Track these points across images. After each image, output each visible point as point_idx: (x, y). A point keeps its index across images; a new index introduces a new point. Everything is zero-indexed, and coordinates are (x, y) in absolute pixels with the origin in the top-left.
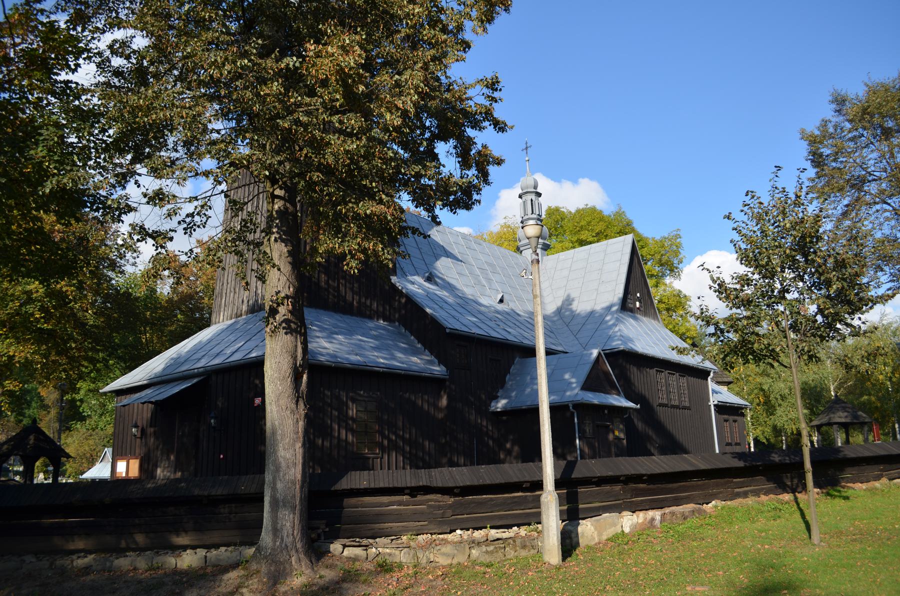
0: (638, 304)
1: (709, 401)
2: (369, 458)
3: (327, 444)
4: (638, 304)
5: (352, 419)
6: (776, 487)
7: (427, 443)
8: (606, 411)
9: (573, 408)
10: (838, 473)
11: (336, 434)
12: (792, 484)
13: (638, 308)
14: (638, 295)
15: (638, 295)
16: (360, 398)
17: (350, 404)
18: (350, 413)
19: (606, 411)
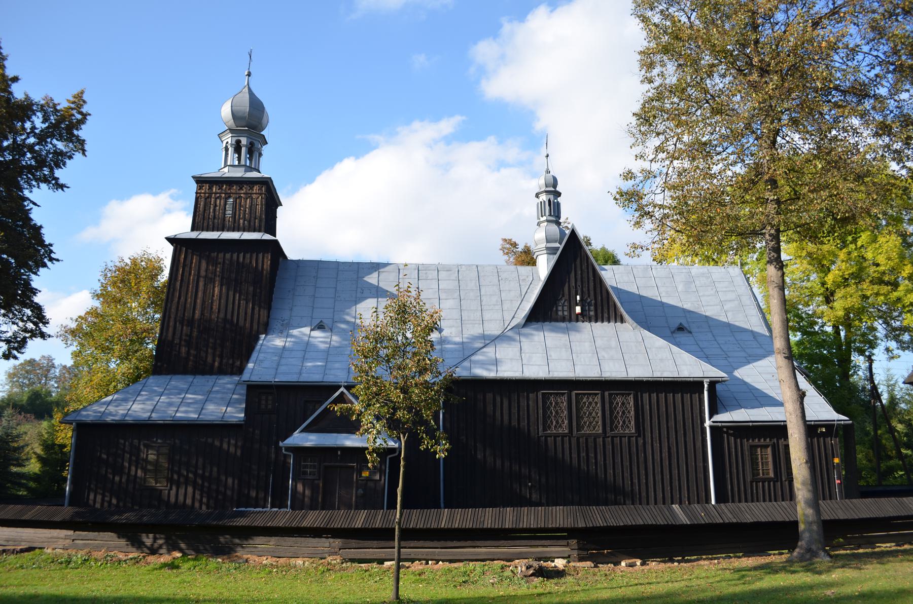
0: (578, 309)
1: (703, 421)
2: (157, 490)
3: (117, 479)
4: (578, 309)
5: (143, 459)
6: (127, 545)
7: (223, 478)
9: (285, 451)
10: (237, 541)
11: (127, 471)
12: (152, 545)
13: (579, 314)
14: (578, 298)
15: (578, 298)
16: (154, 445)
17: (142, 447)
18: (142, 454)
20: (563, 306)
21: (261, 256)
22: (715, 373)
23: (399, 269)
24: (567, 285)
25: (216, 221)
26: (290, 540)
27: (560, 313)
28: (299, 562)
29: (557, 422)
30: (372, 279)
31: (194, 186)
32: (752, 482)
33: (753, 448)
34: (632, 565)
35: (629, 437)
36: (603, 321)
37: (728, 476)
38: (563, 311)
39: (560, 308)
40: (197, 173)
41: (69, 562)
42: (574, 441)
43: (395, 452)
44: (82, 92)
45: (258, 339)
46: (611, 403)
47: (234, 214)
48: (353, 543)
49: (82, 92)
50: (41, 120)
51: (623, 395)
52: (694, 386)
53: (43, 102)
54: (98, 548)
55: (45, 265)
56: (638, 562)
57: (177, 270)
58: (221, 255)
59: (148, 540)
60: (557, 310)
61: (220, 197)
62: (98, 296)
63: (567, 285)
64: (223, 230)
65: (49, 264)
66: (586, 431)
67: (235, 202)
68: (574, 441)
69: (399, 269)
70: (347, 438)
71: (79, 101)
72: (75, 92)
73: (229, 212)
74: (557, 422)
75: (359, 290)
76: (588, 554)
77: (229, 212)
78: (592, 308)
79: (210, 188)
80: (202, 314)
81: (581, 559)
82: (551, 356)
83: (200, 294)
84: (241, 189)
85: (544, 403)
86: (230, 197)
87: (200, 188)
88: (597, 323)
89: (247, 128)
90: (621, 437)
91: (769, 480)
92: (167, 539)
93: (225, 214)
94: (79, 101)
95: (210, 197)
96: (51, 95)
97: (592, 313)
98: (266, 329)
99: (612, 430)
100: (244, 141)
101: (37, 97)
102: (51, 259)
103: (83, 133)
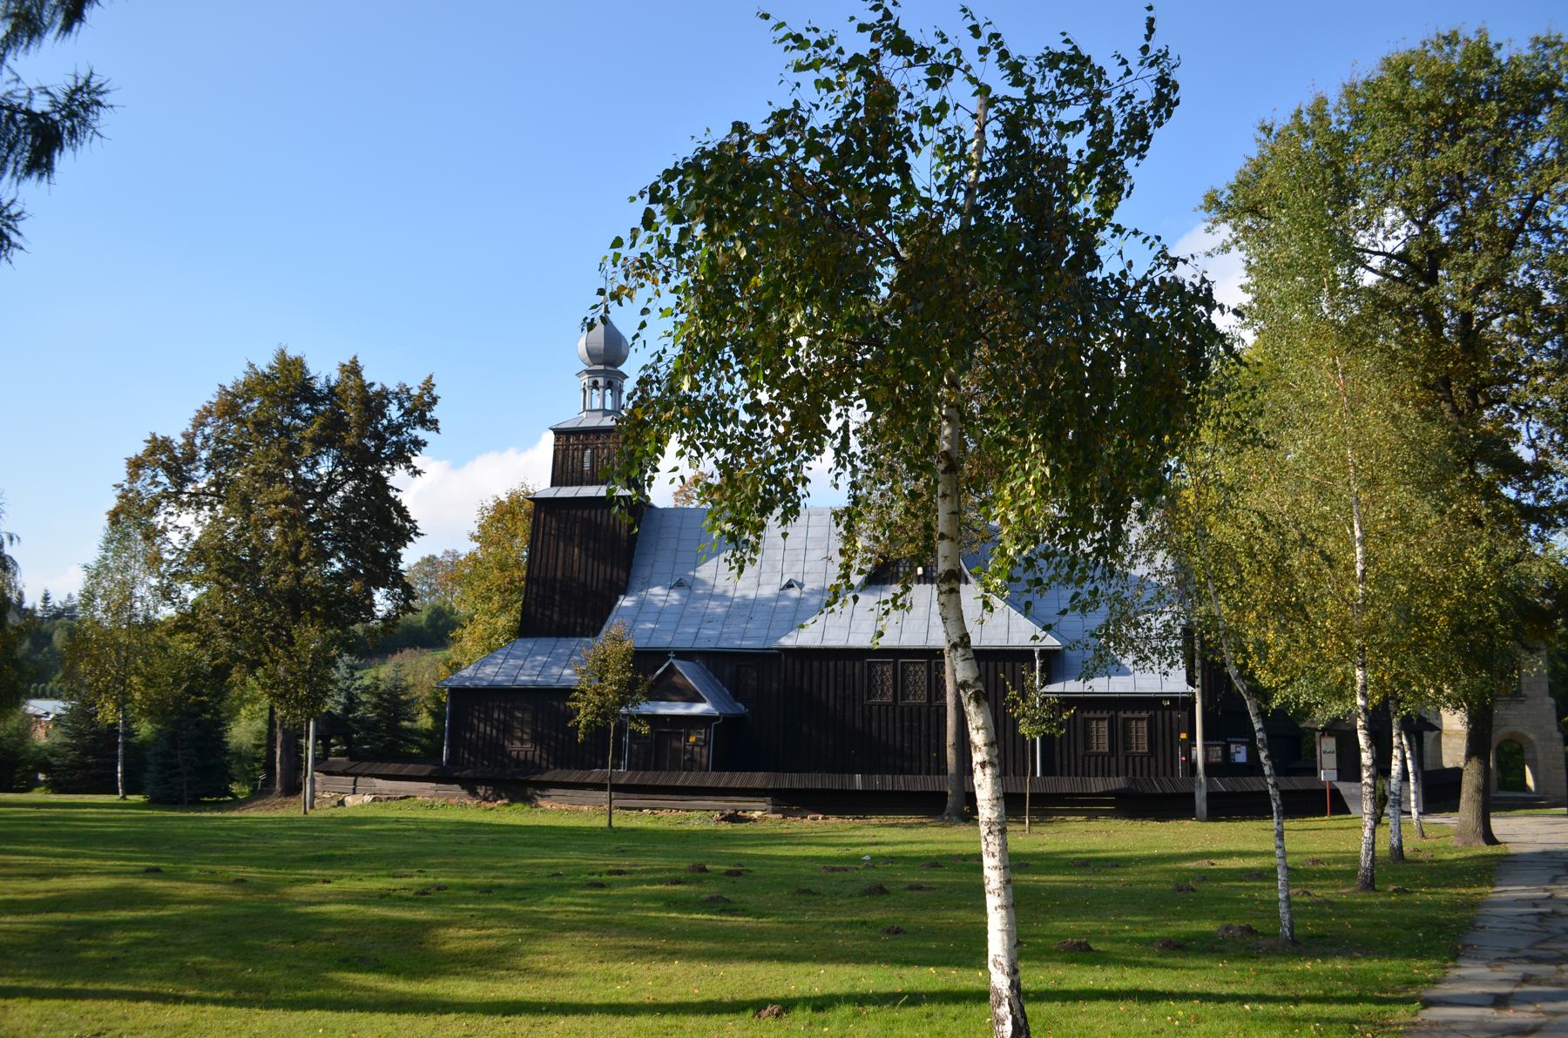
22: (1051, 642)
26: (581, 792)
28: (586, 808)
29: (882, 690)
31: (551, 436)
32: (1083, 757)
33: (1087, 722)
34: (815, 819)
37: (1057, 749)
40: (554, 424)
41: (432, 806)
42: (898, 711)
44: (431, 377)
45: (617, 599)
47: (592, 466)
48: (622, 795)
49: (431, 377)
50: (396, 407)
52: (1024, 655)
53: (397, 390)
54: (453, 797)
55: (411, 540)
56: (820, 817)
58: (579, 513)
59: (481, 791)
61: (577, 449)
62: (474, 538)
64: (581, 482)
65: (415, 538)
66: (911, 700)
67: (592, 453)
68: (898, 711)
71: (428, 386)
72: (424, 378)
73: (587, 465)
74: (882, 690)
77: (587, 465)
79: (568, 439)
80: (564, 571)
81: (774, 812)
83: (561, 554)
84: (598, 438)
85: (870, 671)
86: (586, 448)
87: (557, 439)
89: (602, 367)
91: (1104, 755)
92: (494, 790)
94: (428, 386)
95: (567, 449)
96: (404, 381)
98: (625, 592)
100: (601, 381)
101: (392, 387)
102: (417, 534)
103: (435, 413)
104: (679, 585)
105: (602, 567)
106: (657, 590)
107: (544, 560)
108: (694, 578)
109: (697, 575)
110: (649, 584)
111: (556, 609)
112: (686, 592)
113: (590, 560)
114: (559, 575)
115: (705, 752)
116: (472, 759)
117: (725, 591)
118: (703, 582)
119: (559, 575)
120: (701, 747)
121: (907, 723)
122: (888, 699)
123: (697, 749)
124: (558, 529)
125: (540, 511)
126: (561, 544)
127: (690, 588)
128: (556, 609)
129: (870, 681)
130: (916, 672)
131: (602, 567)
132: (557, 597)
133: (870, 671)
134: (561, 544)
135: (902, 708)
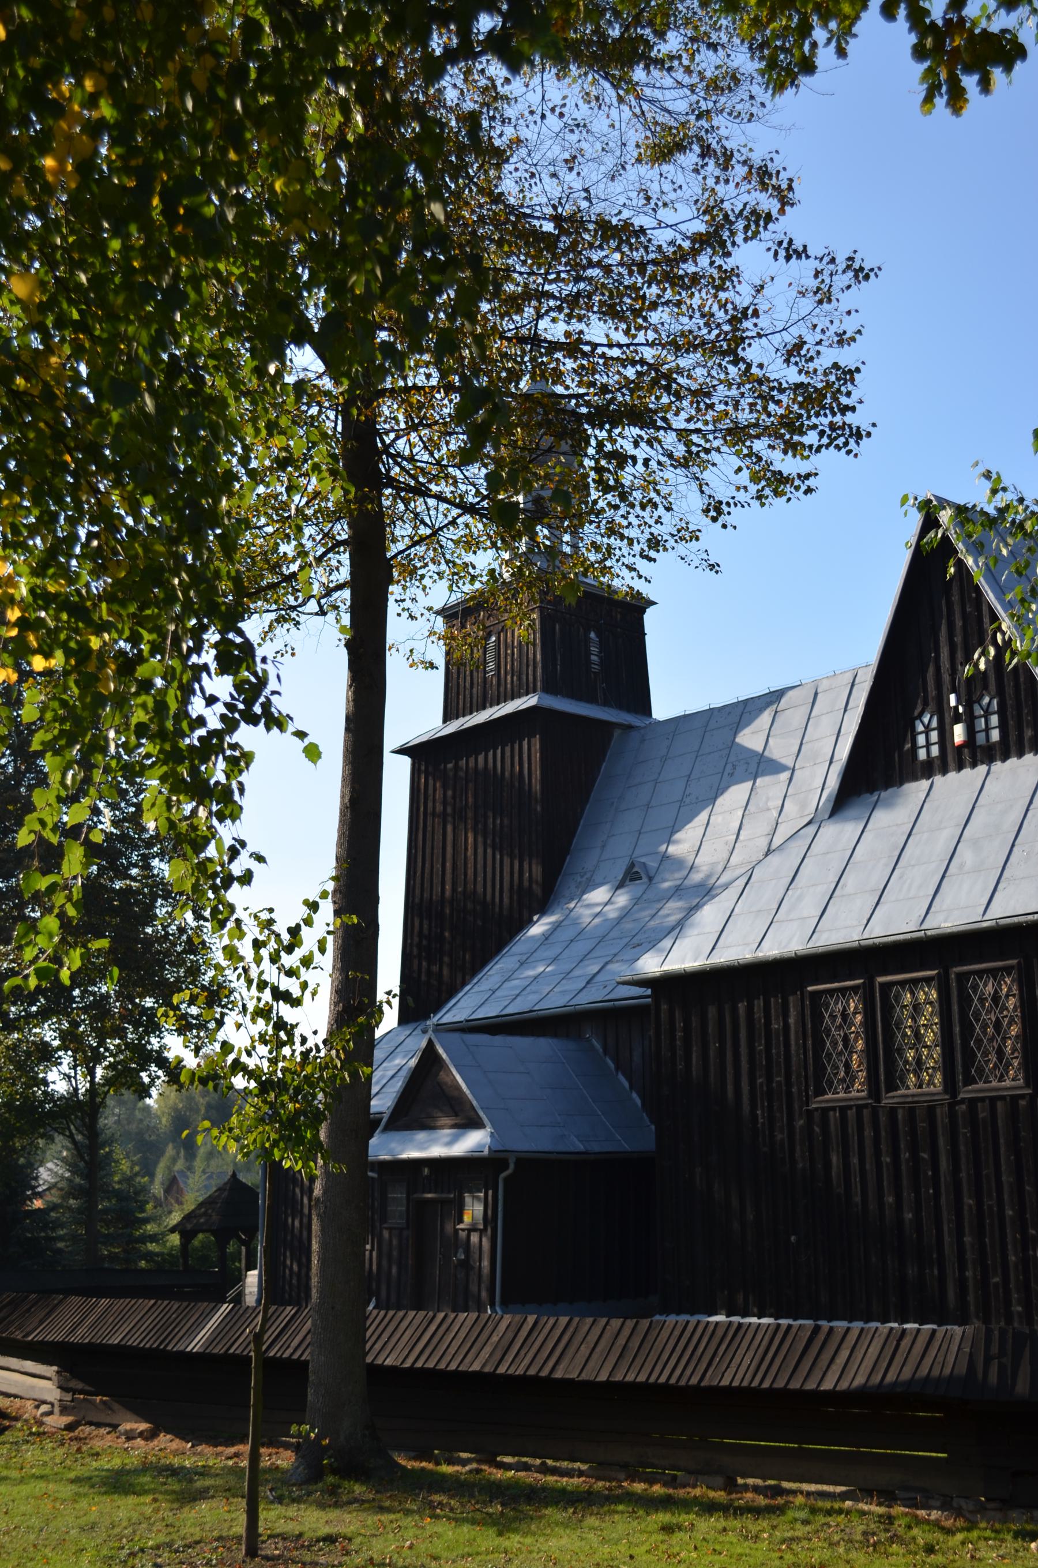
0: (959, 733)
4: (959, 733)
8: (426, 1171)
19: (426, 1171)
20: (928, 730)
21: (525, 743)
23: (816, 694)
24: (931, 670)
25: (475, 690)
27: (922, 754)
30: (751, 738)
35: (1015, 1098)
36: (1020, 754)
38: (928, 745)
39: (921, 740)
42: (883, 1119)
43: (507, 1168)
46: (965, 1001)
51: (993, 973)
57: (418, 809)
60: (915, 748)
63: (931, 670)
67: (499, 638)
68: (883, 1119)
69: (816, 694)
70: (434, 1141)
75: (729, 767)
76: (72, 1401)
78: (994, 720)
80: (454, 889)
82: (845, 885)
86: (489, 635)
88: (1009, 762)
90: (993, 1100)
93: (485, 672)
97: (995, 735)
99: (969, 1080)
104: (631, 875)
105: (507, 861)
106: (599, 895)
107: (427, 865)
108: (665, 857)
109: (672, 849)
110: (591, 885)
111: (446, 959)
112: (638, 887)
113: (489, 851)
114: (448, 893)
115: (486, 1243)
116: (295, 1267)
117: (709, 876)
118: (678, 863)
119: (448, 893)
120: (482, 1232)
121: (905, 1155)
122: (859, 1090)
123: (474, 1238)
124: (445, 803)
125: (419, 771)
126: (449, 828)
127: (650, 879)
128: (446, 959)
129: (819, 1044)
130: (917, 1008)
131: (507, 861)
132: (447, 934)
133: (818, 1018)
134: (449, 828)
135: (892, 1111)
